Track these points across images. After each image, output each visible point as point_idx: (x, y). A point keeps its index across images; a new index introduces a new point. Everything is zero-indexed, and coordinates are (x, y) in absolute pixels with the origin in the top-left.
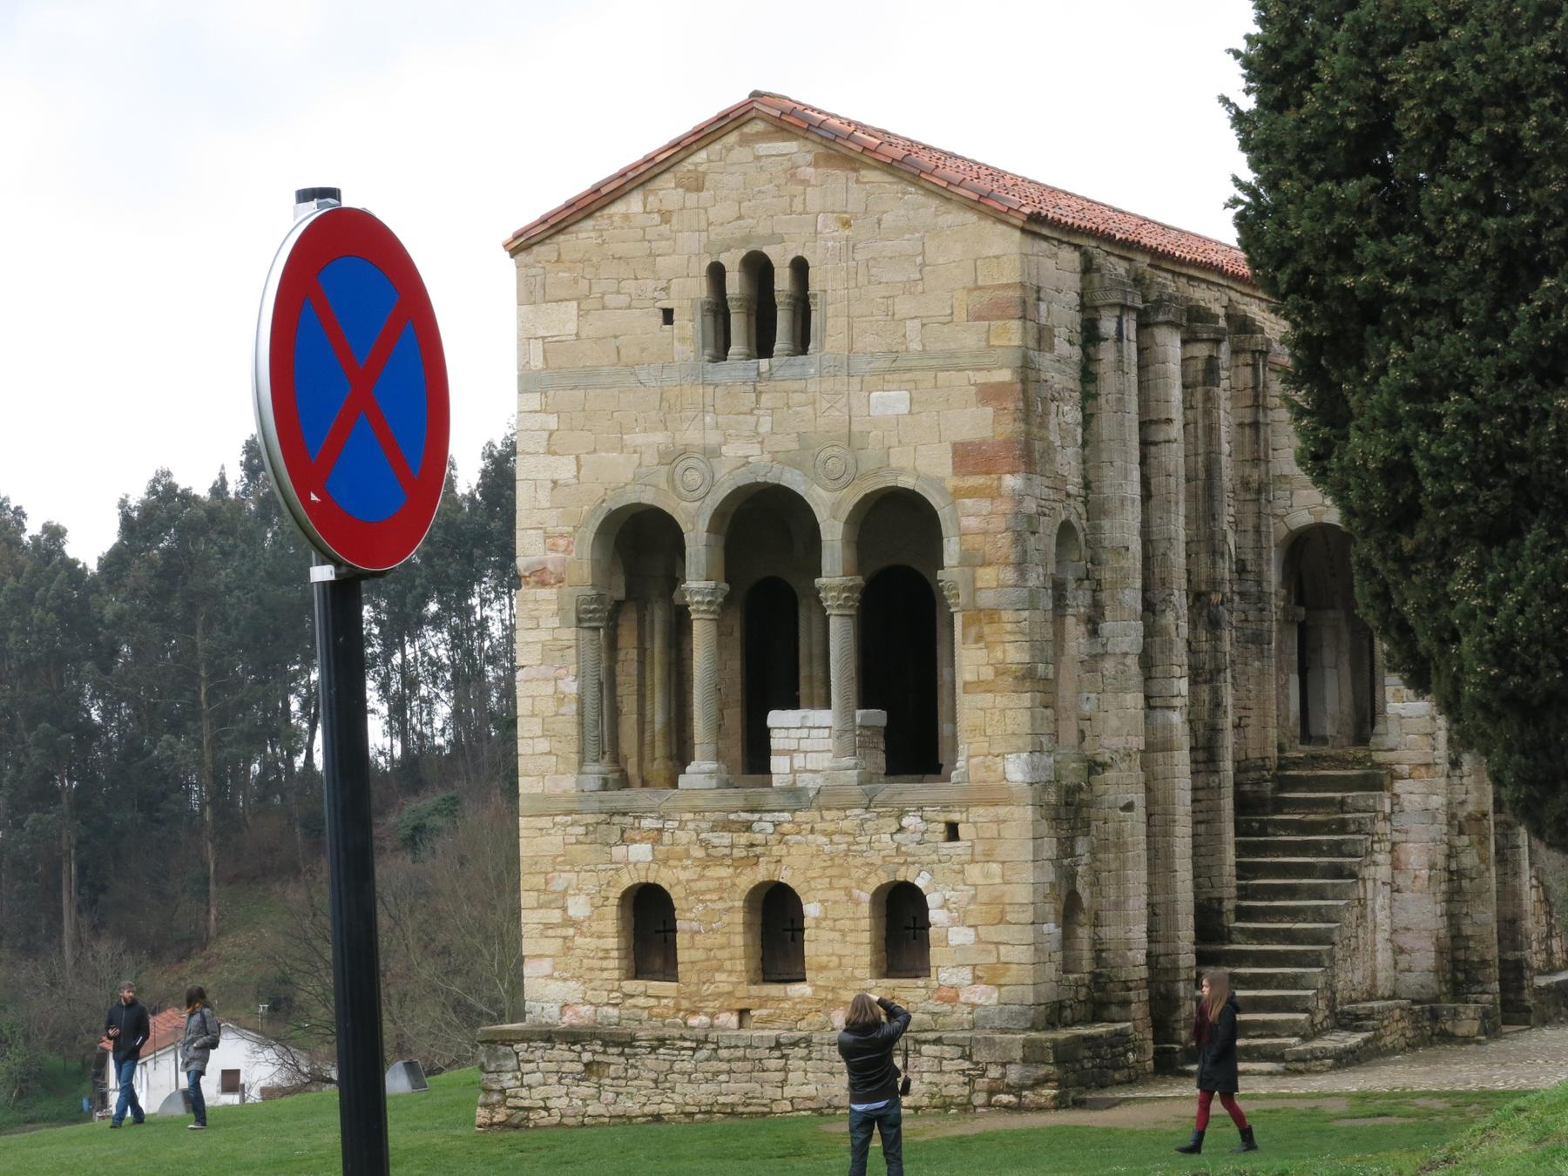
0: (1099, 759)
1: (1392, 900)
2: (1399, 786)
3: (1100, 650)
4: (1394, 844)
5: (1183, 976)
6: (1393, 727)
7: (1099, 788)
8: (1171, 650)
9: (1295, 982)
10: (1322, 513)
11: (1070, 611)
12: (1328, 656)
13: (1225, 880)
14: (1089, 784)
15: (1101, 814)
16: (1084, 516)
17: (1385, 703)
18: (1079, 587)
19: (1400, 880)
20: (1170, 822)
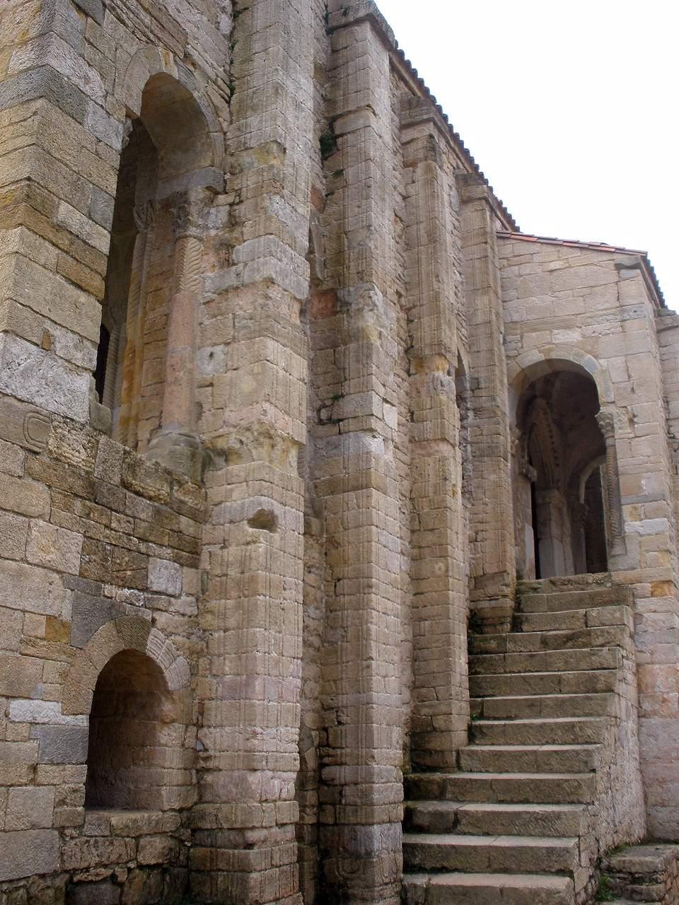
0: (221, 444)
1: (640, 725)
2: (642, 605)
3: (231, 280)
4: (638, 665)
5: (379, 813)
6: (632, 546)
7: (216, 492)
8: (369, 356)
9: (544, 825)
10: (550, 350)
11: (192, 231)
12: (555, 530)
13: (454, 690)
14: (201, 483)
15: (219, 533)
16: (225, 114)
17: (621, 522)
18: (211, 201)
19: (646, 706)
20: (364, 586)
